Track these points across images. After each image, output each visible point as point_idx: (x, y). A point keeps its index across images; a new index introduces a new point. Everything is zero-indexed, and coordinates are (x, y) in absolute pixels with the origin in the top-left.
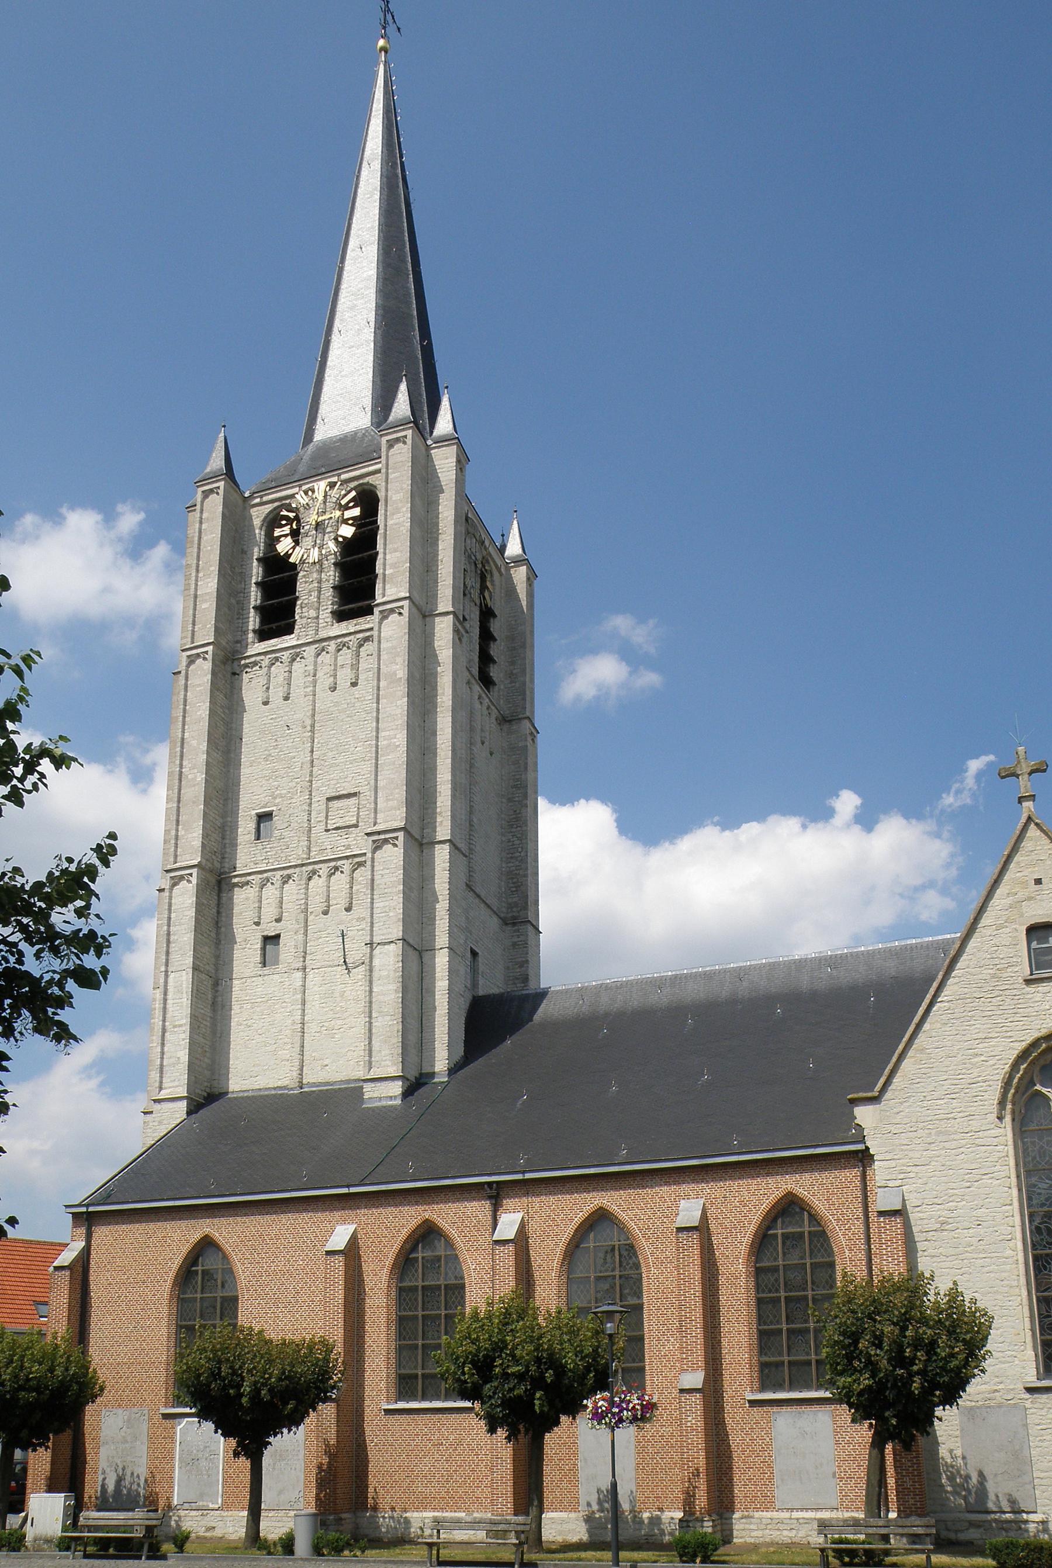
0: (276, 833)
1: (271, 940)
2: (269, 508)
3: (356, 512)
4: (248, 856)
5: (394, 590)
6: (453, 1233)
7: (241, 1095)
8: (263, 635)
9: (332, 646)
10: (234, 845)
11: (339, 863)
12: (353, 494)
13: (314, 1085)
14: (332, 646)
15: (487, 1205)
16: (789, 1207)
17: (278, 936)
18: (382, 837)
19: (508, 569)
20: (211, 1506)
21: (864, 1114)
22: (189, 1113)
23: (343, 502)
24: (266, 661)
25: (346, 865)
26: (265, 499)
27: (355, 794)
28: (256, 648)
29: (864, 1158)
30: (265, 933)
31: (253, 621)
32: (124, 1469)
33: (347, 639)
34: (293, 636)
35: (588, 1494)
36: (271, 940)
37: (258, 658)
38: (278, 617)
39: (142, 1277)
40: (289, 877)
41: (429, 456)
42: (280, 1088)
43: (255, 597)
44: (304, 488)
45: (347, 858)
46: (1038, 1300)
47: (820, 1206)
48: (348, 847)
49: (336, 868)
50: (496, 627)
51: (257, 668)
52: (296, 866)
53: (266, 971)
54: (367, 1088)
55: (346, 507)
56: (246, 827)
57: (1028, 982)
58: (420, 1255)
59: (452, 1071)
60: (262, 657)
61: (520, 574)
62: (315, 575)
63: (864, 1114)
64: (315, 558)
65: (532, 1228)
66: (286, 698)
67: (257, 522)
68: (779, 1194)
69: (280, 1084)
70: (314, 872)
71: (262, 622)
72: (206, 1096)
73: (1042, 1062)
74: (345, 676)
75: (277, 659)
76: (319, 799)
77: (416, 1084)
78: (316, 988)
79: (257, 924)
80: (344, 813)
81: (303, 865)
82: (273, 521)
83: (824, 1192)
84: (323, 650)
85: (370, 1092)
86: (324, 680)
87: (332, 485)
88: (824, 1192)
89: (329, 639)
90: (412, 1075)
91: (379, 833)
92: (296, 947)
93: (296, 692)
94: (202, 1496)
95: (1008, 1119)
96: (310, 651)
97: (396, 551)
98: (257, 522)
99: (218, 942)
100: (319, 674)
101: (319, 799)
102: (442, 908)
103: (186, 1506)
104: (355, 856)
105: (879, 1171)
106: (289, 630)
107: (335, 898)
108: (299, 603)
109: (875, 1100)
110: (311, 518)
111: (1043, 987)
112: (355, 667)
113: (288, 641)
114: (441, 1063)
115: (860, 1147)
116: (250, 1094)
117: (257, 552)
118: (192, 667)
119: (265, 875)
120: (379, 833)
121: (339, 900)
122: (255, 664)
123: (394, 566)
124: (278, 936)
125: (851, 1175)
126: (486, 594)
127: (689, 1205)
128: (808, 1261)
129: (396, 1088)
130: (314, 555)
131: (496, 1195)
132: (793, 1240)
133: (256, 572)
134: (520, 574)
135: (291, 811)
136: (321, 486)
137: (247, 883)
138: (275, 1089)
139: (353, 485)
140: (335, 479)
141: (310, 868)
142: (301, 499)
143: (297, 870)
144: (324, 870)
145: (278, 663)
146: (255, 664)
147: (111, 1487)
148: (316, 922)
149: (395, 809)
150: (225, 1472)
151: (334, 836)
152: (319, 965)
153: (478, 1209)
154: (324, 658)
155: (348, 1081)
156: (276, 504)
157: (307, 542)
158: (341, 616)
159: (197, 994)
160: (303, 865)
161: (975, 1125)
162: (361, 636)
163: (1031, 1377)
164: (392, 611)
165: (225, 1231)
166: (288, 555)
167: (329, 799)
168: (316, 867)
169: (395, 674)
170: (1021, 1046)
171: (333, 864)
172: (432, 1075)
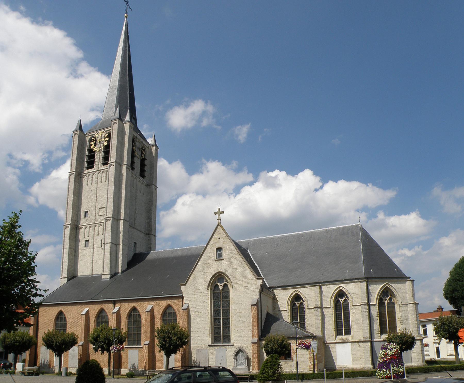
1: (87, 241)
2: (90, 137)
3: (108, 139)
4: (83, 221)
6: (107, 310)
8: (88, 168)
9: (101, 172)
10: (80, 219)
14: (101, 172)
15: (113, 305)
16: (169, 306)
19: (151, 147)
21: (183, 288)
22: (67, 281)
24: (87, 175)
28: (86, 171)
29: (182, 297)
31: (86, 165)
35: (130, 365)
36: (87, 241)
38: (91, 165)
41: (123, 126)
43: (86, 159)
46: (214, 328)
47: (174, 307)
50: (146, 163)
53: (86, 248)
54: (103, 276)
55: (106, 138)
56: (82, 214)
57: (215, 260)
58: (101, 315)
59: (122, 272)
61: (153, 149)
63: (183, 288)
64: (99, 149)
65: (121, 310)
67: (87, 140)
68: (167, 304)
71: (88, 165)
72: (72, 276)
73: (218, 278)
74: (104, 179)
76: (97, 208)
77: (113, 275)
80: (103, 212)
82: (91, 140)
83: (175, 303)
85: (103, 277)
88: (175, 303)
90: (113, 274)
93: (94, 182)
95: (209, 290)
96: (97, 173)
98: (87, 140)
99: (76, 241)
101: (97, 208)
102: (121, 235)
106: (93, 167)
109: (185, 285)
110: (98, 140)
111: (218, 262)
113: (93, 170)
114: (120, 271)
117: (87, 148)
121: (101, 232)
122: (85, 175)
123: (113, 154)
125: (181, 300)
126: (143, 155)
127: (149, 306)
129: (108, 277)
130: (98, 149)
131: (115, 303)
132: (170, 314)
133: (87, 153)
134: (153, 149)
136: (101, 132)
142: (97, 135)
147: (43, 362)
148: (96, 237)
153: (111, 305)
154: (100, 175)
157: (97, 146)
159: (70, 254)
163: (210, 344)
165: (65, 309)
166: (93, 149)
172: (118, 273)
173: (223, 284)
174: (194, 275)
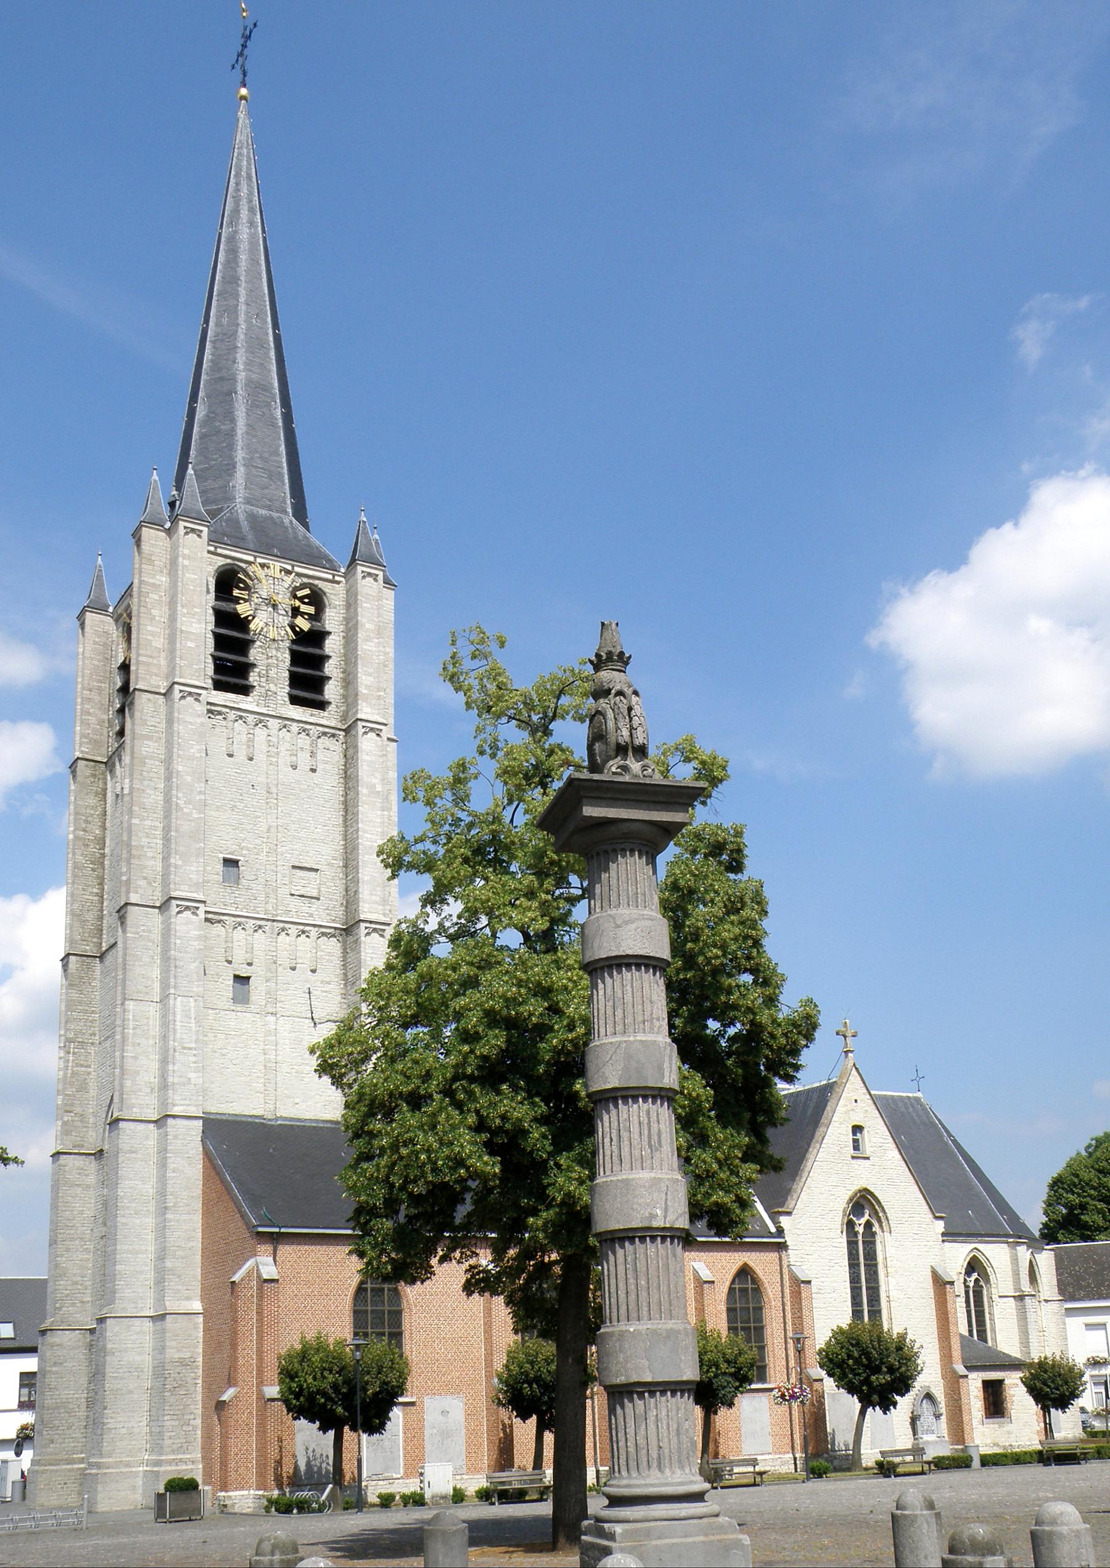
0: (243, 881)
2: (221, 561)
5: (368, 710)
7: (218, 1117)
9: (295, 727)
11: (307, 928)
12: (307, 591)
13: (286, 1119)
17: (248, 978)
18: (373, 926)
20: (395, 1476)
23: (300, 594)
24: (232, 715)
25: (314, 932)
26: (219, 551)
27: (317, 870)
29: (782, 1247)
30: (237, 973)
32: (314, 1451)
33: (307, 727)
34: (249, 699)
36: (242, 980)
37: (224, 710)
39: (325, 1291)
40: (260, 927)
42: (257, 1117)
44: (259, 560)
45: (314, 926)
48: (311, 915)
49: (303, 932)
51: (220, 717)
52: (268, 920)
60: (227, 710)
62: (274, 652)
66: (251, 759)
68: (740, 1263)
69: (254, 1113)
70: (283, 930)
75: (241, 717)
78: (285, 1033)
79: (230, 962)
80: (309, 884)
81: (274, 921)
83: (761, 1263)
84: (285, 727)
86: (285, 759)
87: (288, 572)
88: (761, 1263)
89: (293, 720)
91: (371, 922)
92: (268, 993)
93: (260, 757)
94: (387, 1469)
97: (370, 675)
100: (282, 748)
103: (374, 1477)
104: (321, 926)
105: (793, 1256)
107: (301, 958)
108: (256, 670)
112: (313, 754)
115: (782, 1240)
116: (224, 1118)
118: (182, 701)
119: (239, 919)
120: (371, 922)
122: (220, 713)
123: (367, 687)
124: (248, 978)
125: (774, 1255)
128: (751, 1306)
135: (257, 866)
137: (219, 922)
138: (251, 1116)
139: (305, 580)
140: (289, 568)
141: (281, 925)
143: (269, 923)
144: (294, 930)
145: (240, 721)
146: (220, 713)
147: (302, 1467)
148: (285, 975)
149: (376, 903)
150: (405, 1449)
151: (297, 901)
152: (288, 1014)
155: (317, 1121)
156: (229, 561)
158: (295, 700)
160: (274, 921)
161: (832, 1235)
162: (321, 729)
164: (372, 729)
167: (294, 867)
168: (287, 926)
169: (374, 786)
170: (850, 1193)
171: (302, 927)
173: (863, 1221)
174: (809, 1188)
